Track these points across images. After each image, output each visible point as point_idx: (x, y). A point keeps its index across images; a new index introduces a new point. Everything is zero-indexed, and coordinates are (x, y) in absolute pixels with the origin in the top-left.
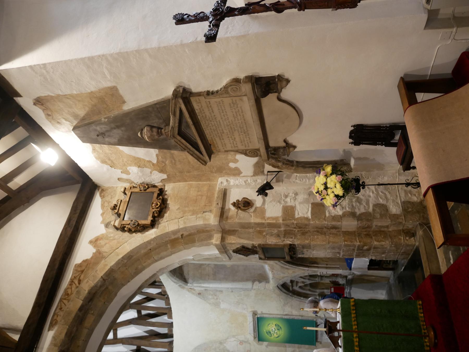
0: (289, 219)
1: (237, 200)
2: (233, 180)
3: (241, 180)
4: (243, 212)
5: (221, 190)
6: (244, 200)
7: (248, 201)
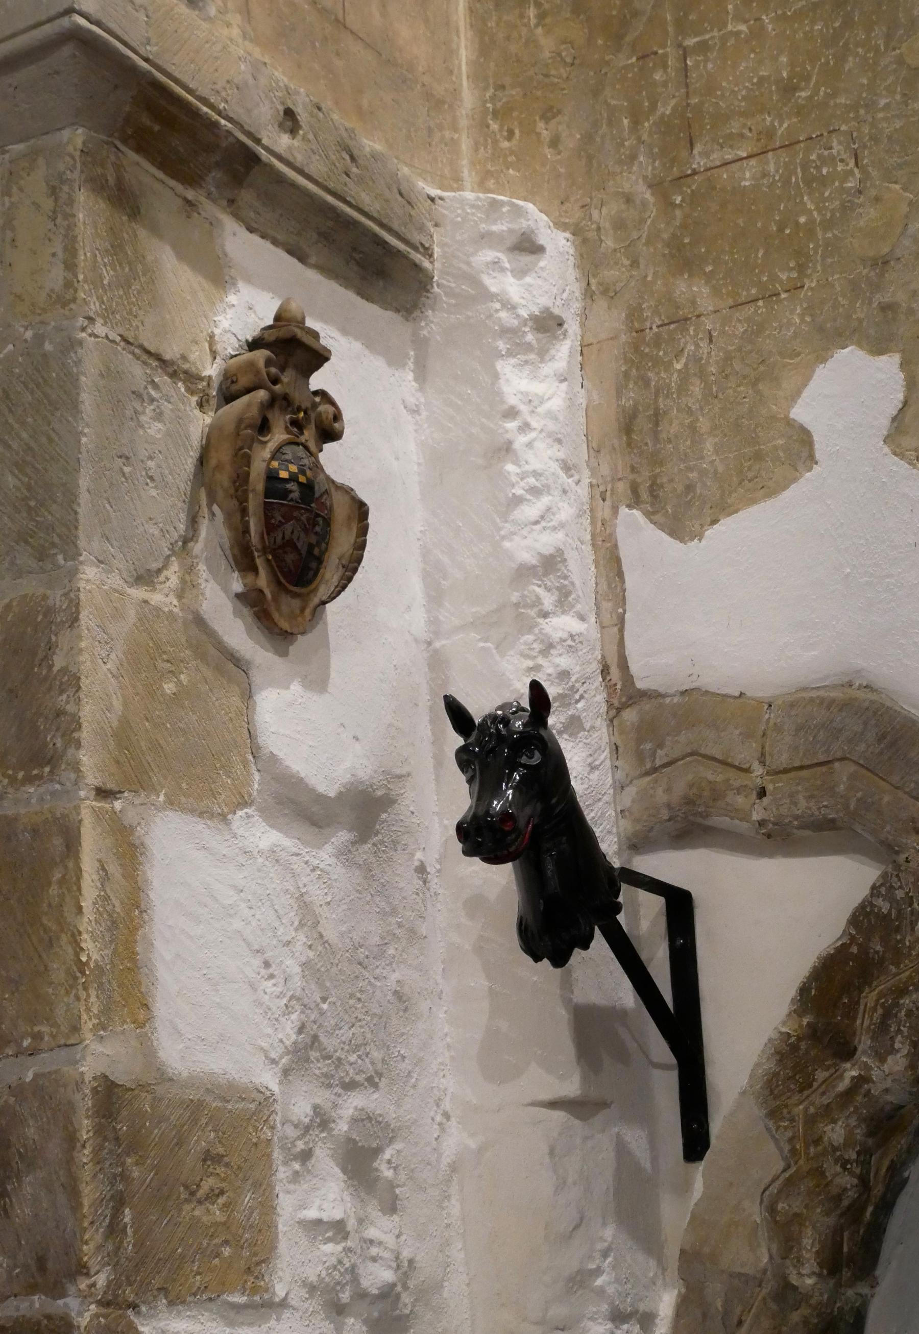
0: (119, 1202)
1: (337, 417)
2: (556, 404)
3: (566, 511)
4: (189, 464)
5: (421, 228)
6: (341, 510)
7: (331, 574)
